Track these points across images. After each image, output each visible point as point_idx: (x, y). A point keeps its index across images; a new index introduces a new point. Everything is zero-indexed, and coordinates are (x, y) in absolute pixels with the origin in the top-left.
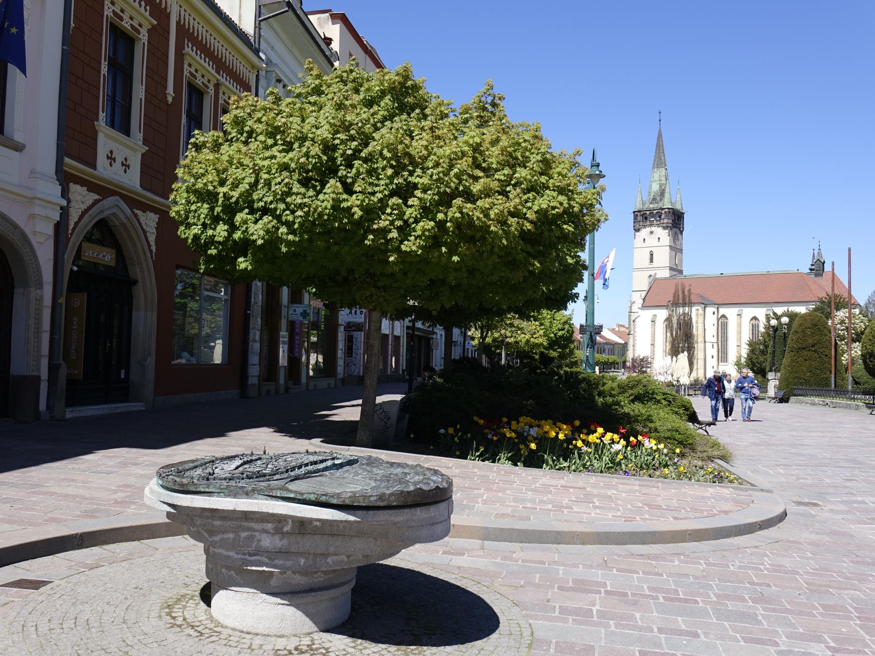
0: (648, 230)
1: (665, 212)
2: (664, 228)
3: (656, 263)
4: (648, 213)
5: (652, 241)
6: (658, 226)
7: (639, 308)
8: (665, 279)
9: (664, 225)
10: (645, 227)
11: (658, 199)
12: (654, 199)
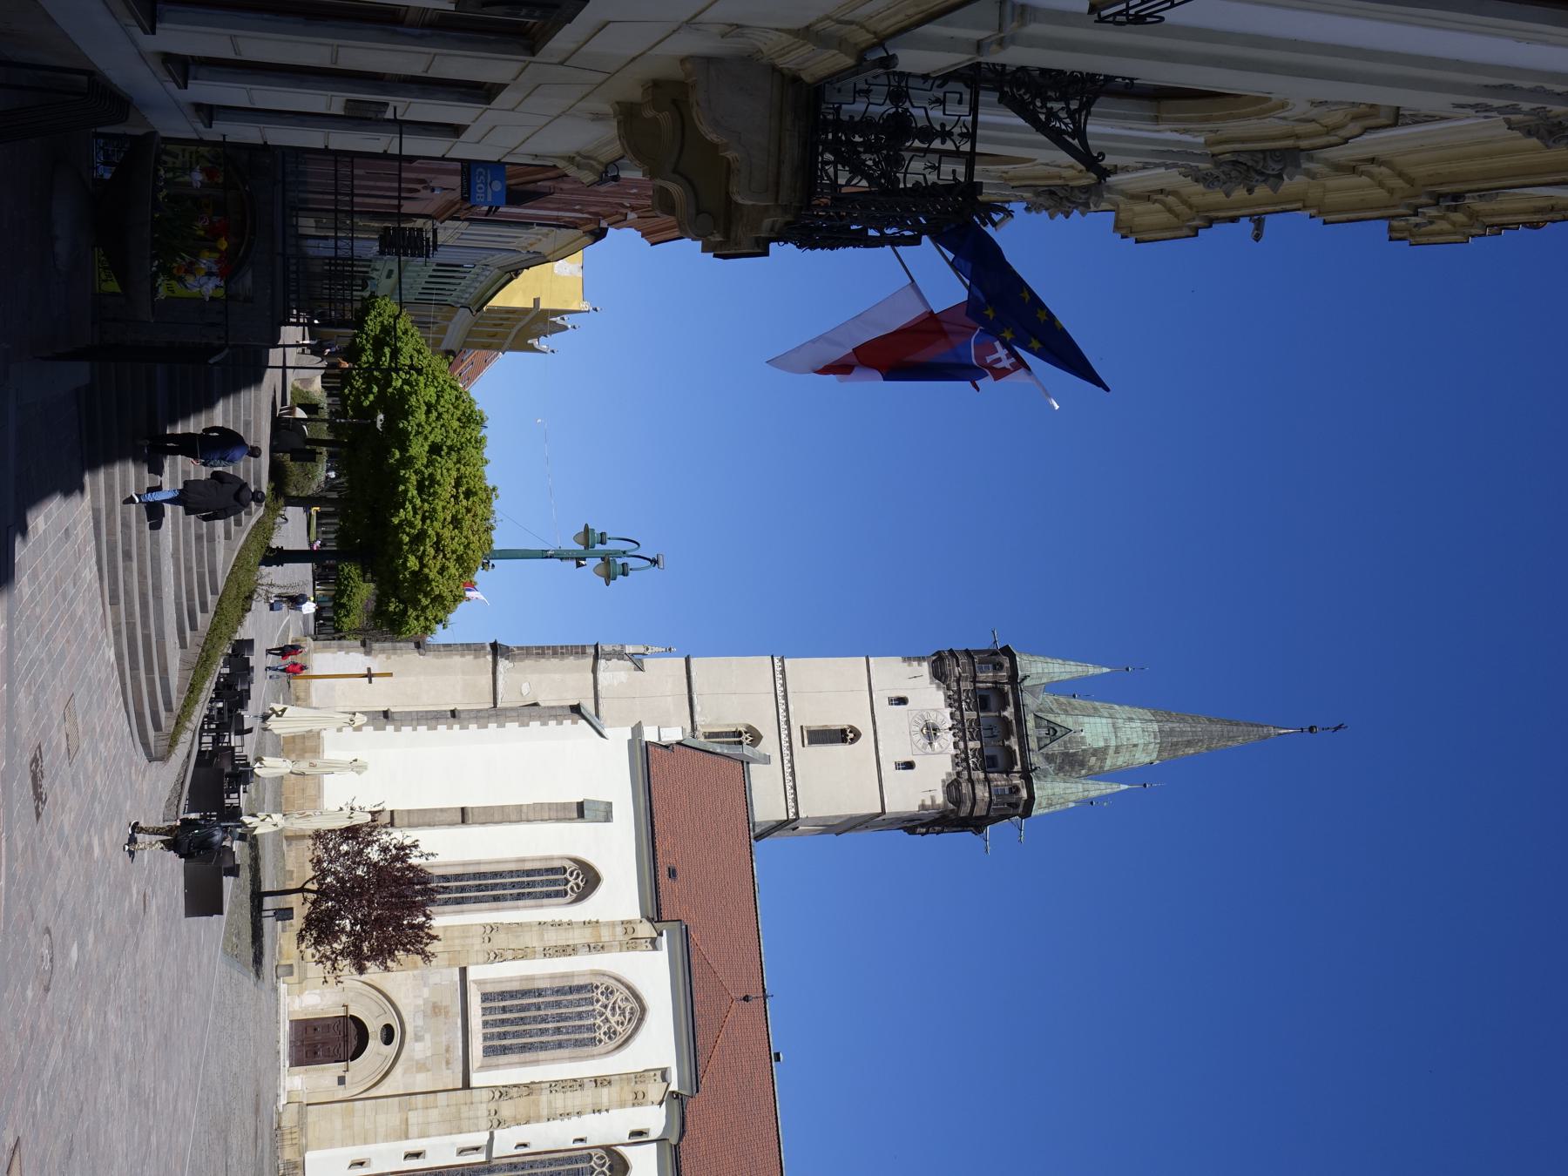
0: (944, 718)
1: (1015, 790)
2: (952, 787)
3: (811, 758)
4: (1009, 713)
6: (960, 760)
7: (637, 730)
8: (748, 805)
9: (965, 788)
10: (954, 701)
11: (1055, 747)
12: (1053, 731)
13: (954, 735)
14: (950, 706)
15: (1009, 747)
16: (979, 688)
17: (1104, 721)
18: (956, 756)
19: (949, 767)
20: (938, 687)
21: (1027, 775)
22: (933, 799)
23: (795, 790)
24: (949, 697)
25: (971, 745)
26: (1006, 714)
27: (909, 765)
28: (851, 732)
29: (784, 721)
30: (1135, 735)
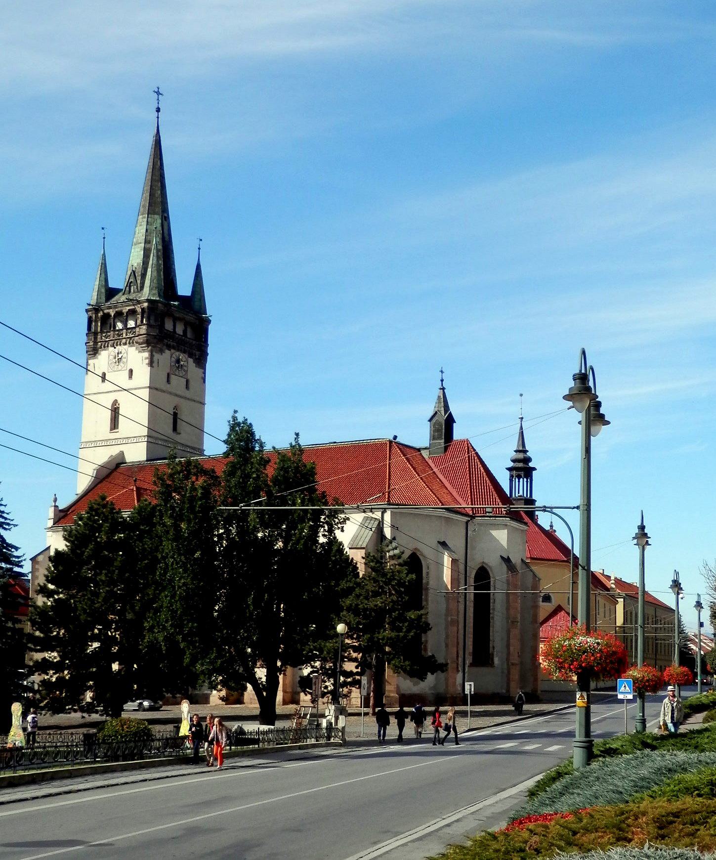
4: (112, 313)
5: (119, 377)
13: (120, 345)
14: (108, 346)
15: (127, 313)
16: (101, 330)
17: (133, 250)
18: (129, 343)
19: (134, 348)
20: (100, 354)
21: (139, 302)
22: (146, 359)
23: (135, 437)
24: (104, 347)
25: (124, 335)
26: (113, 315)
27: (131, 371)
28: (116, 405)
29: (106, 443)
30: (142, 231)
